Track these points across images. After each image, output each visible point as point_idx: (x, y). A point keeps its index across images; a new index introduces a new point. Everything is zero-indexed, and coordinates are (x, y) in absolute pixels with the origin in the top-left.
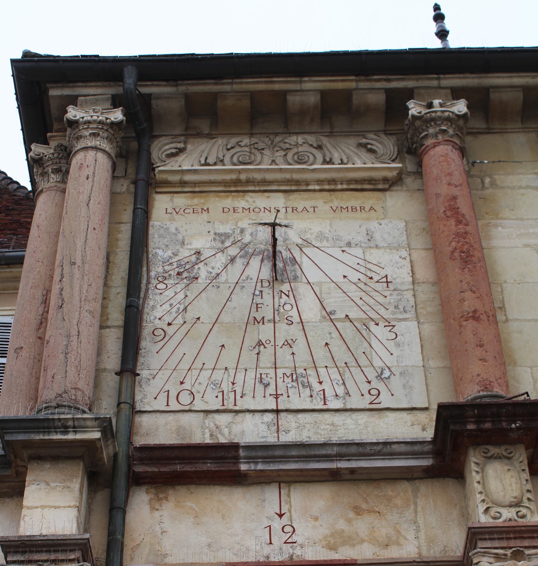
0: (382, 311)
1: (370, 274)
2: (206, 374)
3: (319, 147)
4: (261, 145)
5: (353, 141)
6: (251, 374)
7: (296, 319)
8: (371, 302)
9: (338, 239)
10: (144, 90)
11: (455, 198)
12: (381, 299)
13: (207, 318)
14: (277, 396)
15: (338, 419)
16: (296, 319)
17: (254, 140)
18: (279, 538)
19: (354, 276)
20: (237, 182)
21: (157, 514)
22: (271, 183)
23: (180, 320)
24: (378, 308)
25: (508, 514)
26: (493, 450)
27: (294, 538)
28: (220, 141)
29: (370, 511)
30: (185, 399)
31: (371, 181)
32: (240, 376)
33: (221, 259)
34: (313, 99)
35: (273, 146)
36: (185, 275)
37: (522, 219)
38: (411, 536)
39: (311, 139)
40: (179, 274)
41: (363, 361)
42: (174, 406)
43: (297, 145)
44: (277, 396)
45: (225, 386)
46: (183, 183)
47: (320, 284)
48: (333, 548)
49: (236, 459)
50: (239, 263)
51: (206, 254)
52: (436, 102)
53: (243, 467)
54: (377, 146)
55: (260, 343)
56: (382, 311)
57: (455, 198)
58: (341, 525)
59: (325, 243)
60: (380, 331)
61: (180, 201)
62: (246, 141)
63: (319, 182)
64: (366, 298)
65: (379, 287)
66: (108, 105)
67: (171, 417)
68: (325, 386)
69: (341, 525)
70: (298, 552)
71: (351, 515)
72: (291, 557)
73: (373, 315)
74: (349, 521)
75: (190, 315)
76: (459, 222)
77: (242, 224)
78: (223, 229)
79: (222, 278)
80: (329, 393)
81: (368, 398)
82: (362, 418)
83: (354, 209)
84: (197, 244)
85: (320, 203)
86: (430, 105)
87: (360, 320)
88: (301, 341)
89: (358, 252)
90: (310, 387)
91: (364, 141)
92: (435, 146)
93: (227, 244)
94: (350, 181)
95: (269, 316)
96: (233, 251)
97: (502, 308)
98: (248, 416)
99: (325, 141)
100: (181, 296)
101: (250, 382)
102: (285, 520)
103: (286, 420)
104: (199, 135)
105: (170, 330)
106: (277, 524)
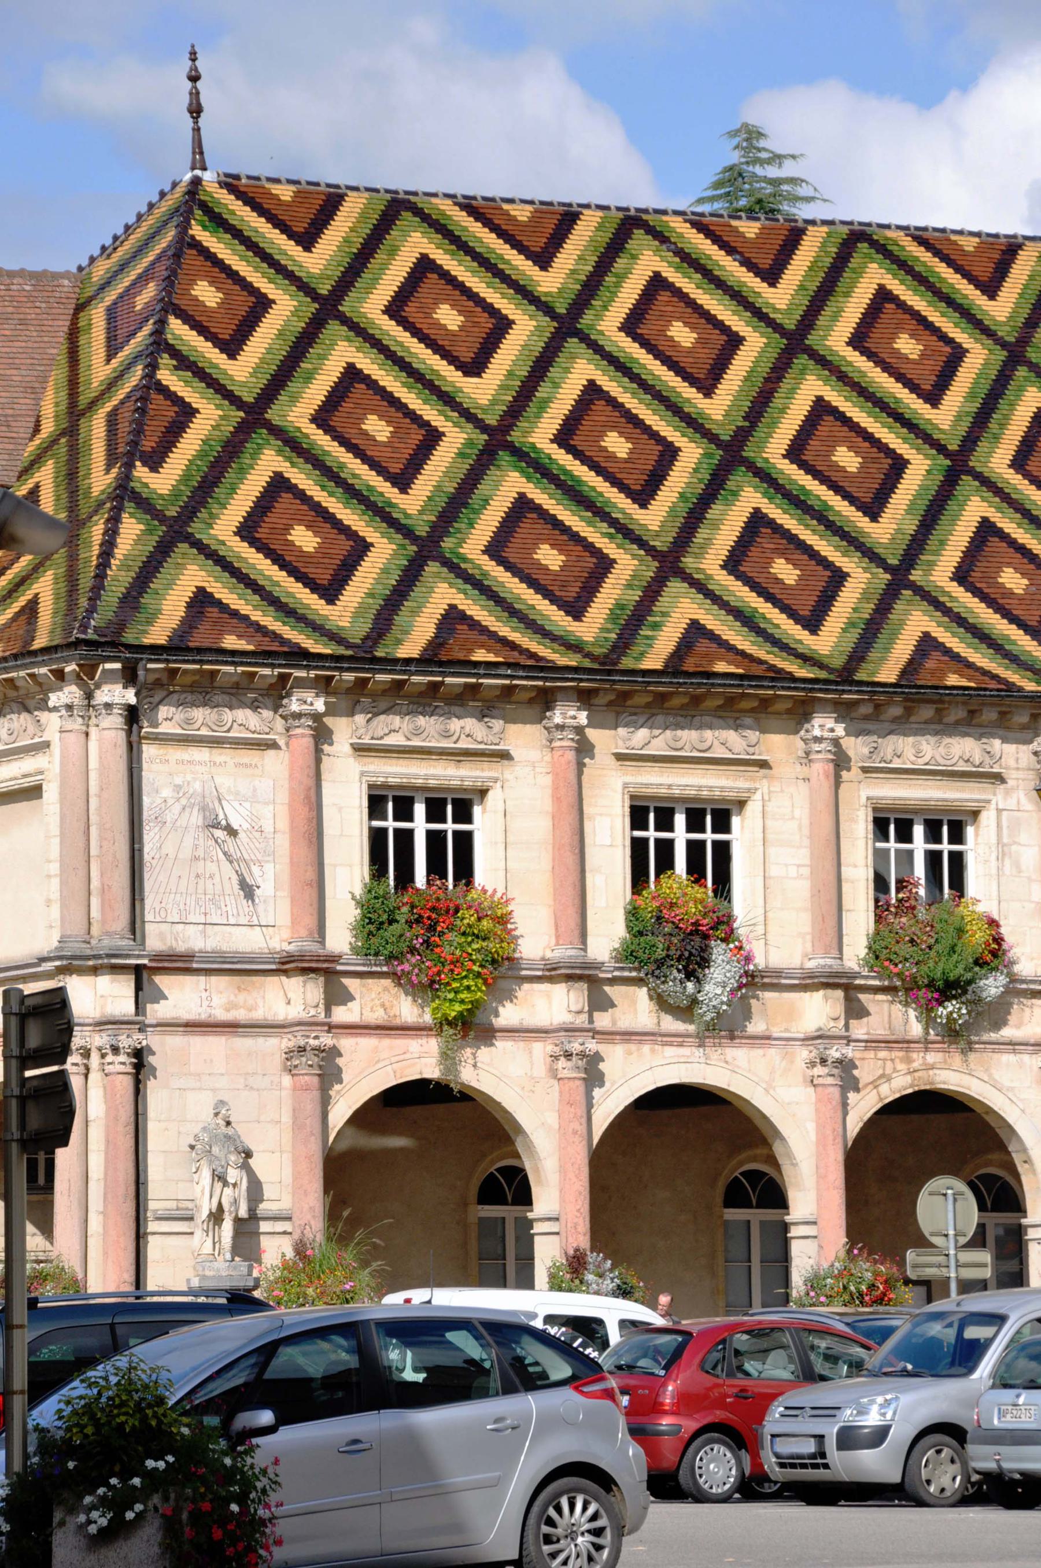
0: (258, 854)
1: (254, 824)
6: (193, 897)
7: (215, 858)
8: (253, 846)
9: (237, 793)
12: (257, 844)
13: (172, 856)
16: (215, 858)
18: (205, 1003)
23: (157, 856)
24: (256, 851)
25: (313, 1012)
30: (163, 914)
33: (177, 808)
36: (159, 819)
37: (334, 782)
40: (156, 818)
42: (158, 919)
44: (205, 914)
45: (182, 907)
50: (188, 810)
51: (170, 802)
55: (198, 876)
56: (258, 854)
58: (232, 998)
59: (232, 798)
64: (251, 844)
67: (156, 925)
68: (229, 908)
69: (232, 998)
70: (213, 1012)
73: (253, 858)
74: (236, 995)
75: (164, 851)
77: (189, 777)
78: (178, 781)
79: (178, 824)
80: (230, 913)
81: (248, 918)
85: (227, 759)
88: (217, 876)
89: (247, 805)
90: (220, 908)
93: (181, 795)
95: (202, 856)
96: (184, 801)
100: (157, 837)
101: (193, 903)
102: (208, 993)
105: (154, 862)
106: (204, 995)
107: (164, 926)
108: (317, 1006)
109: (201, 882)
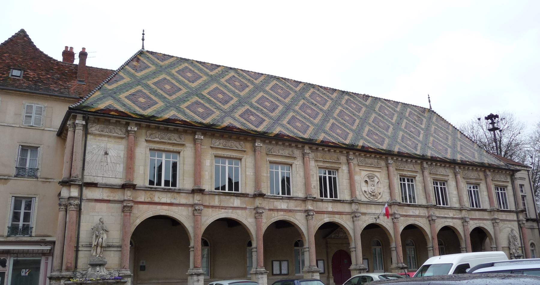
2: (94, 170)
3: (114, 129)
4: (105, 127)
5: (119, 128)
6: (100, 171)
10: (89, 116)
11: (132, 147)
14: (103, 175)
15: (110, 178)
17: (104, 126)
19: (116, 155)
20: (101, 135)
21: (86, 191)
22: (106, 136)
23: (91, 160)
25: (129, 198)
26: (129, 189)
27: (103, 195)
28: (99, 125)
29: (113, 193)
30: (91, 174)
31: (121, 137)
32: (99, 171)
34: (114, 121)
35: (107, 128)
38: (117, 196)
39: (113, 127)
41: (115, 170)
43: (111, 128)
44: (103, 175)
46: (92, 134)
47: (111, 156)
48: (108, 197)
49: (97, 185)
50: (100, 151)
52: (133, 127)
53: (98, 186)
54: (122, 130)
55: (102, 166)
57: (132, 147)
58: (109, 194)
60: (118, 165)
61: (92, 137)
62: (103, 126)
63: (113, 136)
65: (119, 158)
66: (82, 118)
69: (109, 194)
71: (110, 193)
72: (103, 198)
73: (117, 162)
76: (131, 152)
78: (98, 144)
81: (115, 176)
82: (114, 179)
83: (117, 142)
84: (94, 146)
86: (131, 128)
87: (116, 163)
91: (121, 129)
92: (131, 135)
94: (117, 137)
97: (135, 163)
98: (99, 177)
99: (115, 128)
102: (102, 193)
103: (104, 178)
104: (96, 123)
106: (101, 193)
107: (91, 177)
108: (130, 196)
109: (102, 167)
